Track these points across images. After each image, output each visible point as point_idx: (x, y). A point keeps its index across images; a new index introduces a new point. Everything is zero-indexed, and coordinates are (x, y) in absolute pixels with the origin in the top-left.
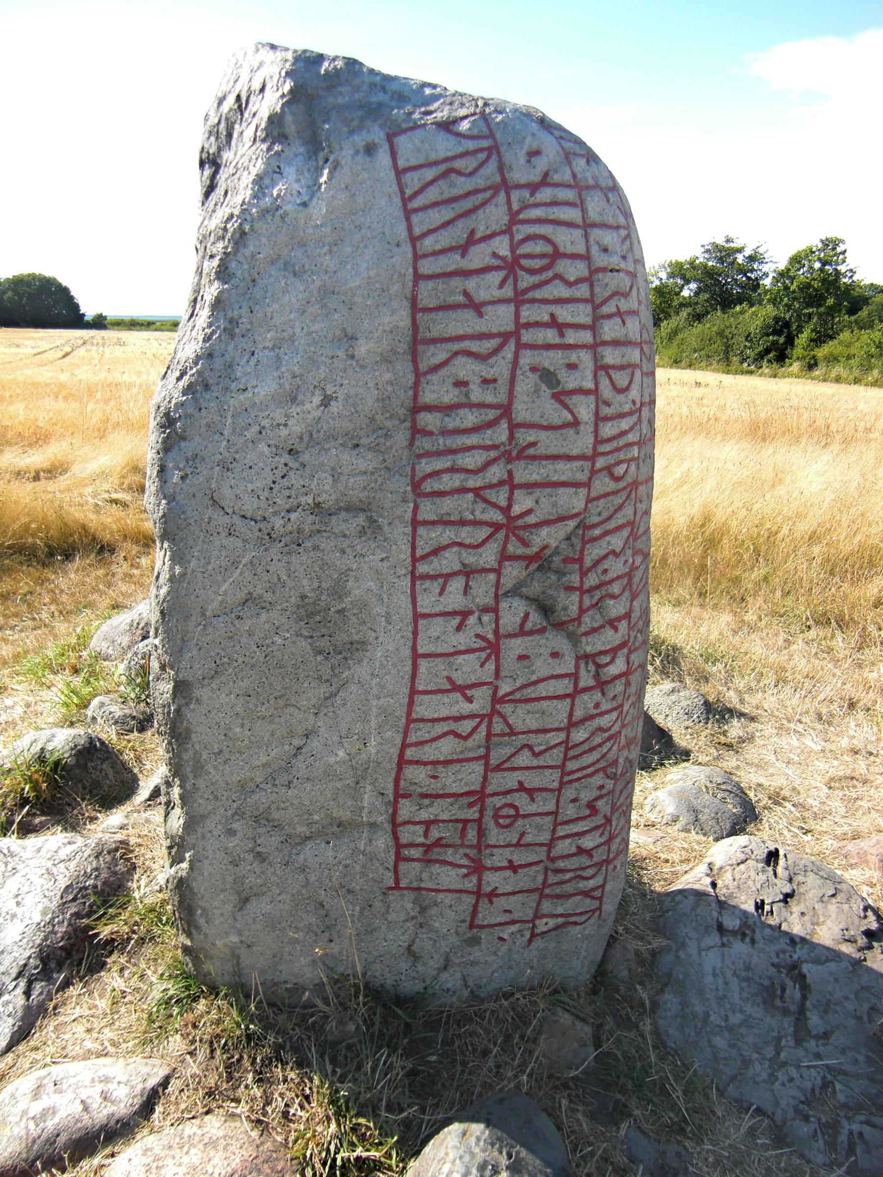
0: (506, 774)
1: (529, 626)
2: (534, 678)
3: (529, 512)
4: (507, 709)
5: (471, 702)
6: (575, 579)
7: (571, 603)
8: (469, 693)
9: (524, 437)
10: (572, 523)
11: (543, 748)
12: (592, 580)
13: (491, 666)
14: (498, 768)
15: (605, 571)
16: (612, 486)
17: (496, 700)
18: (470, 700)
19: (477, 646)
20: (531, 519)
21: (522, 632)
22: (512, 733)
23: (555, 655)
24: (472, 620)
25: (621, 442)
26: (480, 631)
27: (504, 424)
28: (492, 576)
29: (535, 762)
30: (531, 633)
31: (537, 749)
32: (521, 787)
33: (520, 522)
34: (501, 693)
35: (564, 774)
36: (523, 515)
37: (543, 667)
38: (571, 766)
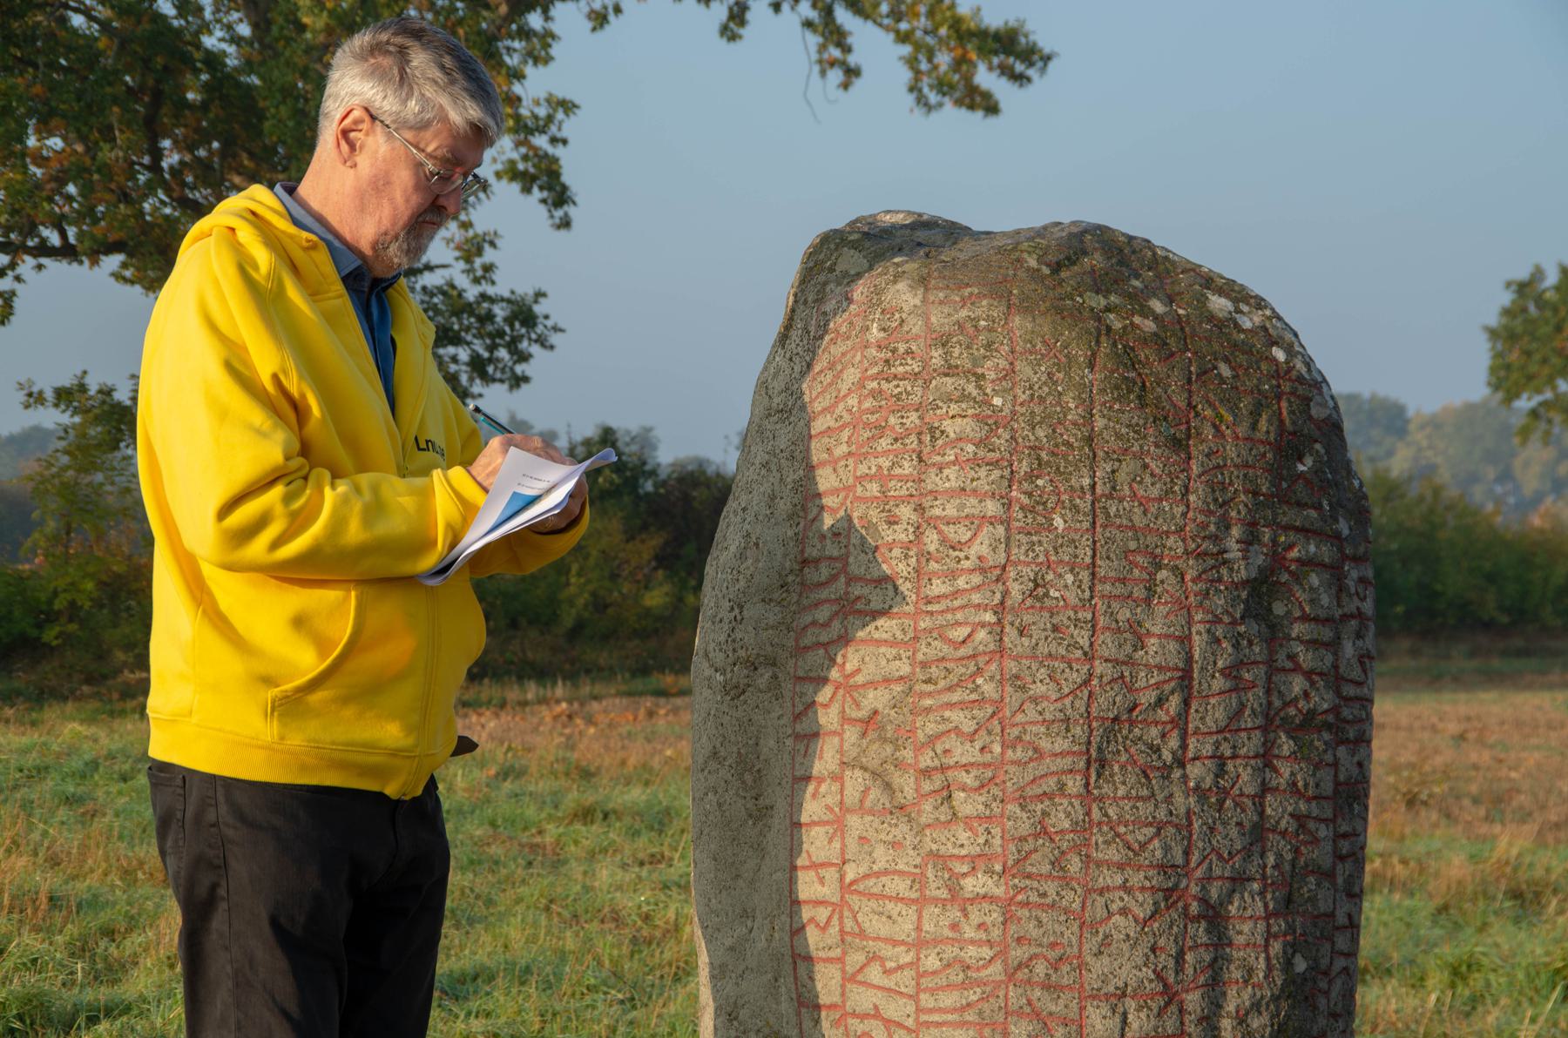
0: (861, 989)
1: (868, 804)
2: (875, 868)
3: (858, 671)
4: (854, 900)
5: (823, 884)
6: (907, 754)
7: (906, 785)
8: (822, 872)
9: (857, 590)
10: (898, 688)
11: (893, 965)
12: (926, 760)
13: (837, 845)
14: (852, 979)
15: (946, 751)
16: (946, 650)
17: (846, 888)
18: (822, 880)
19: (825, 818)
20: (860, 679)
21: (861, 809)
22: (862, 934)
23: (895, 845)
24: (823, 788)
25: (957, 603)
26: (829, 800)
27: (842, 579)
28: (836, 740)
29: (888, 982)
30: (871, 812)
31: (890, 965)
32: (876, 1014)
33: (852, 681)
34: (849, 877)
35: (919, 1010)
36: (853, 674)
37: (882, 857)
38: (926, 1000)
